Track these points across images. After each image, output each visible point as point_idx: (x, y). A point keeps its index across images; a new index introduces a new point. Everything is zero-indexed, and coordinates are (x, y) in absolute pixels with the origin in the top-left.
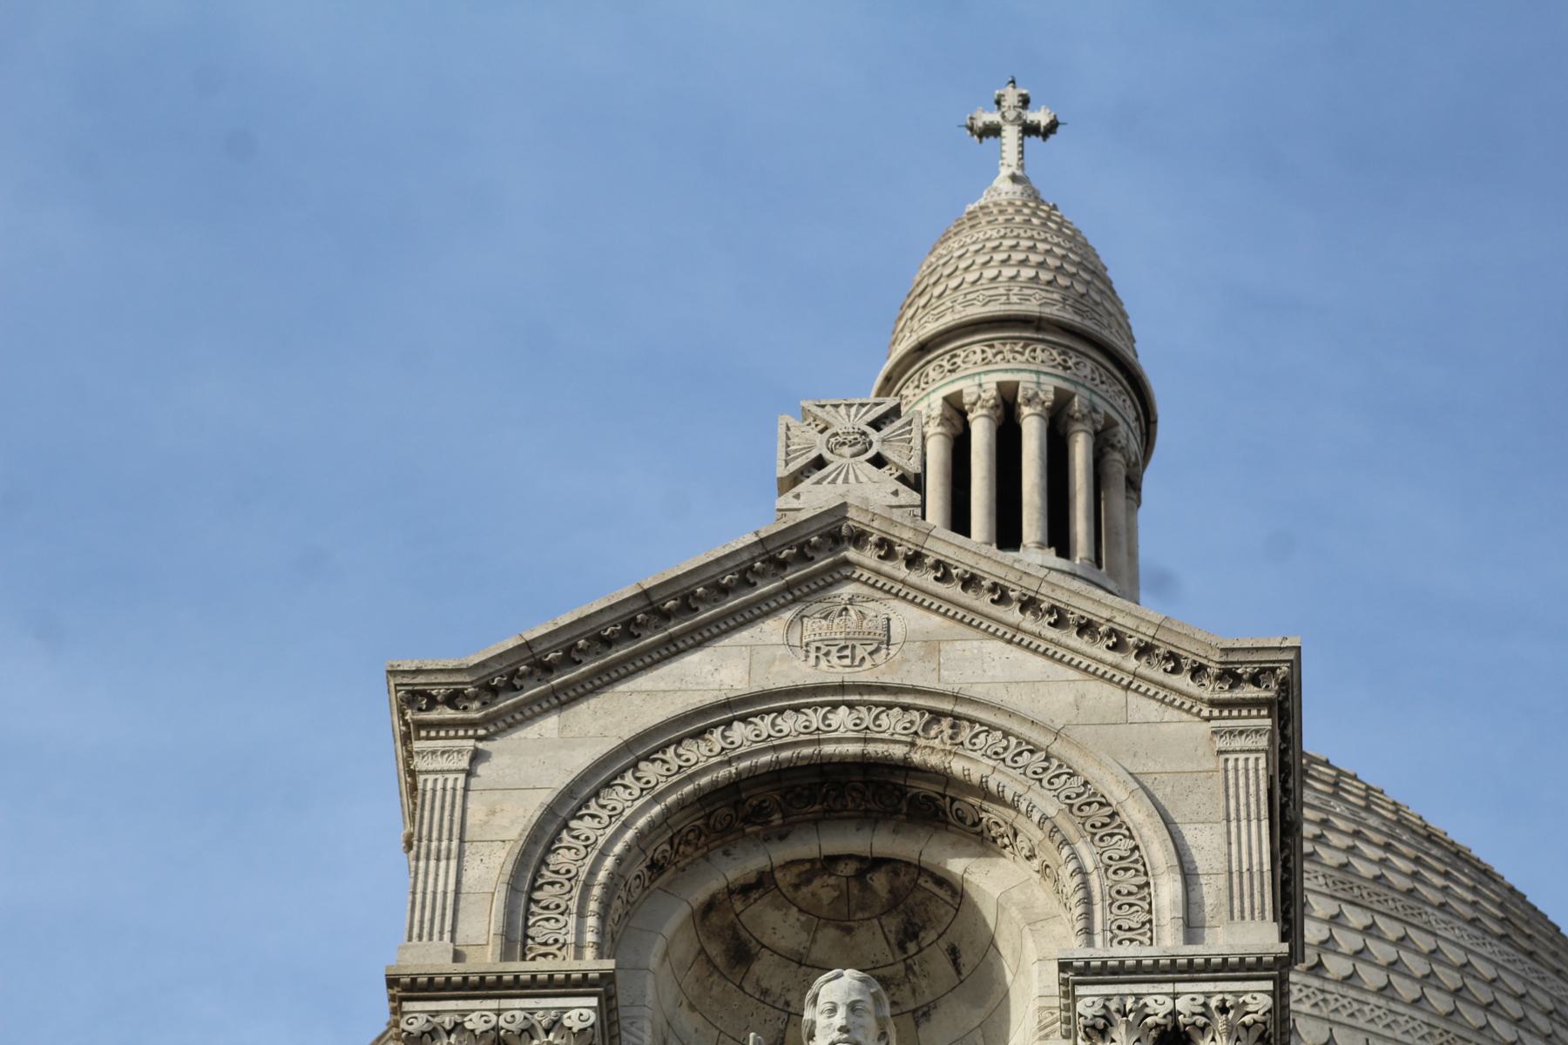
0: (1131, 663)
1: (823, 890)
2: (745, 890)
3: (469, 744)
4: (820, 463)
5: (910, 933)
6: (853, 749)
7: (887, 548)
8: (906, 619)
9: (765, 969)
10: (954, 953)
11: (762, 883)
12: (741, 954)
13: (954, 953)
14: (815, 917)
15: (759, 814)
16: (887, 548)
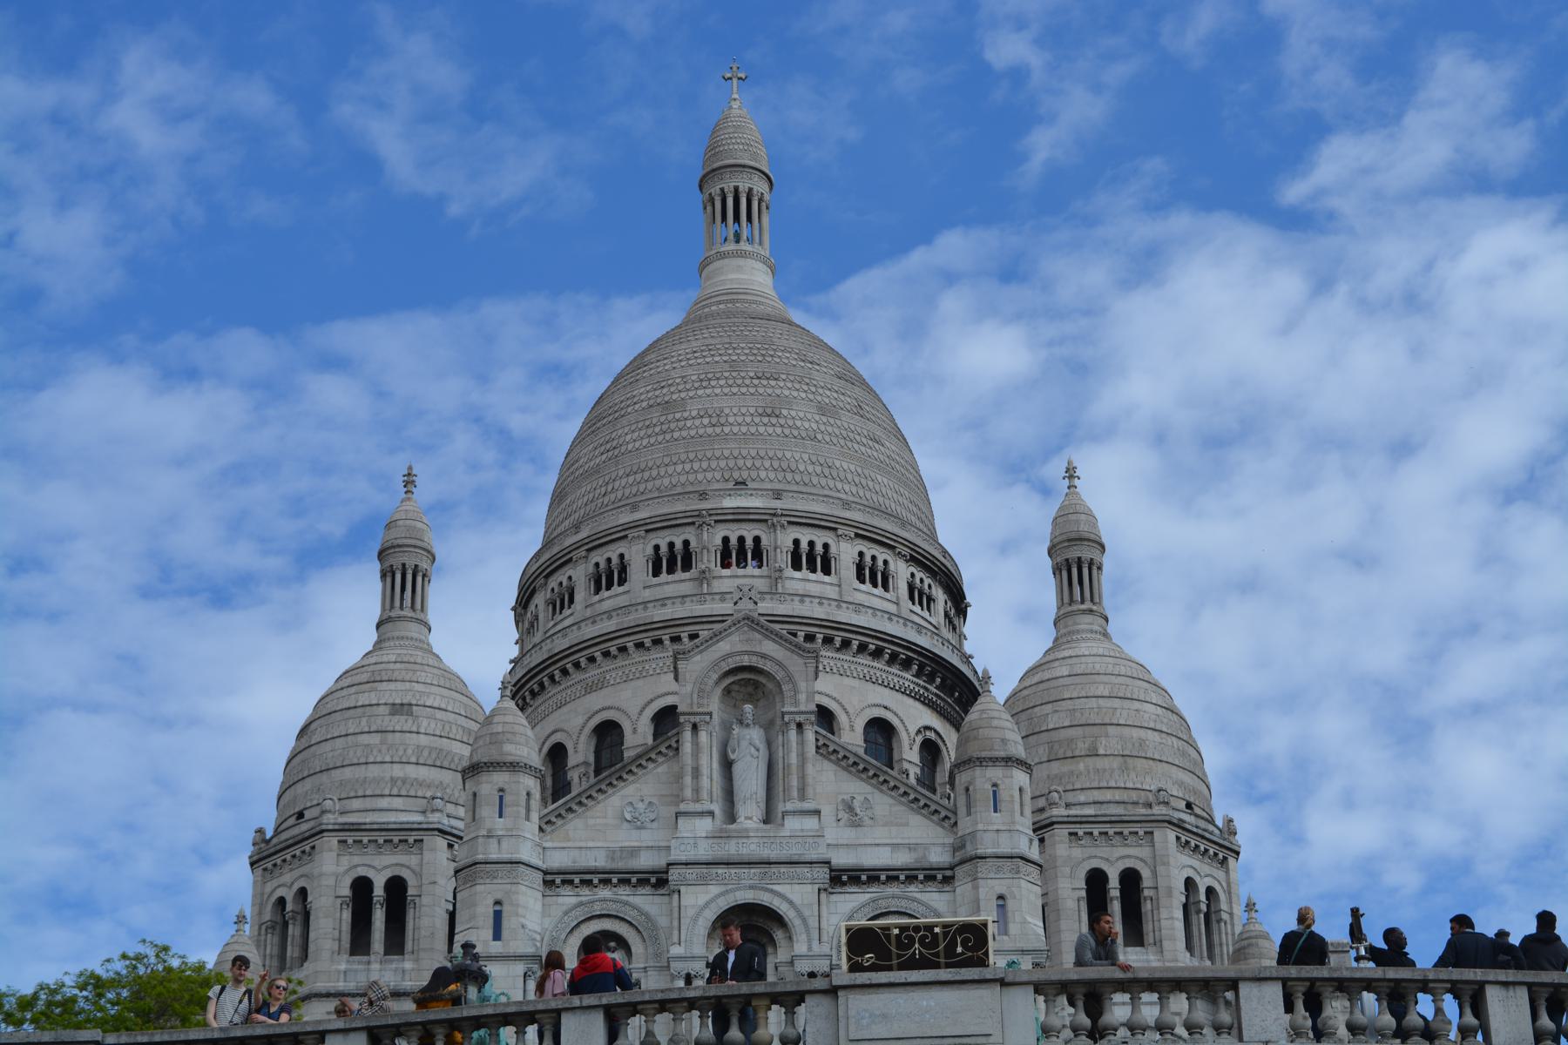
0: (793, 648)
1: (742, 682)
2: (730, 684)
3: (686, 662)
4: (741, 599)
5: (756, 688)
6: (748, 664)
7: (753, 621)
8: (758, 636)
9: (733, 694)
10: (763, 693)
11: (733, 683)
12: (729, 692)
13: (763, 693)
14: (741, 686)
15: (732, 672)
16: (753, 621)
